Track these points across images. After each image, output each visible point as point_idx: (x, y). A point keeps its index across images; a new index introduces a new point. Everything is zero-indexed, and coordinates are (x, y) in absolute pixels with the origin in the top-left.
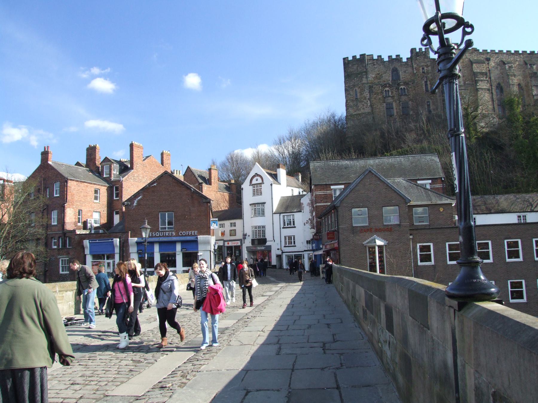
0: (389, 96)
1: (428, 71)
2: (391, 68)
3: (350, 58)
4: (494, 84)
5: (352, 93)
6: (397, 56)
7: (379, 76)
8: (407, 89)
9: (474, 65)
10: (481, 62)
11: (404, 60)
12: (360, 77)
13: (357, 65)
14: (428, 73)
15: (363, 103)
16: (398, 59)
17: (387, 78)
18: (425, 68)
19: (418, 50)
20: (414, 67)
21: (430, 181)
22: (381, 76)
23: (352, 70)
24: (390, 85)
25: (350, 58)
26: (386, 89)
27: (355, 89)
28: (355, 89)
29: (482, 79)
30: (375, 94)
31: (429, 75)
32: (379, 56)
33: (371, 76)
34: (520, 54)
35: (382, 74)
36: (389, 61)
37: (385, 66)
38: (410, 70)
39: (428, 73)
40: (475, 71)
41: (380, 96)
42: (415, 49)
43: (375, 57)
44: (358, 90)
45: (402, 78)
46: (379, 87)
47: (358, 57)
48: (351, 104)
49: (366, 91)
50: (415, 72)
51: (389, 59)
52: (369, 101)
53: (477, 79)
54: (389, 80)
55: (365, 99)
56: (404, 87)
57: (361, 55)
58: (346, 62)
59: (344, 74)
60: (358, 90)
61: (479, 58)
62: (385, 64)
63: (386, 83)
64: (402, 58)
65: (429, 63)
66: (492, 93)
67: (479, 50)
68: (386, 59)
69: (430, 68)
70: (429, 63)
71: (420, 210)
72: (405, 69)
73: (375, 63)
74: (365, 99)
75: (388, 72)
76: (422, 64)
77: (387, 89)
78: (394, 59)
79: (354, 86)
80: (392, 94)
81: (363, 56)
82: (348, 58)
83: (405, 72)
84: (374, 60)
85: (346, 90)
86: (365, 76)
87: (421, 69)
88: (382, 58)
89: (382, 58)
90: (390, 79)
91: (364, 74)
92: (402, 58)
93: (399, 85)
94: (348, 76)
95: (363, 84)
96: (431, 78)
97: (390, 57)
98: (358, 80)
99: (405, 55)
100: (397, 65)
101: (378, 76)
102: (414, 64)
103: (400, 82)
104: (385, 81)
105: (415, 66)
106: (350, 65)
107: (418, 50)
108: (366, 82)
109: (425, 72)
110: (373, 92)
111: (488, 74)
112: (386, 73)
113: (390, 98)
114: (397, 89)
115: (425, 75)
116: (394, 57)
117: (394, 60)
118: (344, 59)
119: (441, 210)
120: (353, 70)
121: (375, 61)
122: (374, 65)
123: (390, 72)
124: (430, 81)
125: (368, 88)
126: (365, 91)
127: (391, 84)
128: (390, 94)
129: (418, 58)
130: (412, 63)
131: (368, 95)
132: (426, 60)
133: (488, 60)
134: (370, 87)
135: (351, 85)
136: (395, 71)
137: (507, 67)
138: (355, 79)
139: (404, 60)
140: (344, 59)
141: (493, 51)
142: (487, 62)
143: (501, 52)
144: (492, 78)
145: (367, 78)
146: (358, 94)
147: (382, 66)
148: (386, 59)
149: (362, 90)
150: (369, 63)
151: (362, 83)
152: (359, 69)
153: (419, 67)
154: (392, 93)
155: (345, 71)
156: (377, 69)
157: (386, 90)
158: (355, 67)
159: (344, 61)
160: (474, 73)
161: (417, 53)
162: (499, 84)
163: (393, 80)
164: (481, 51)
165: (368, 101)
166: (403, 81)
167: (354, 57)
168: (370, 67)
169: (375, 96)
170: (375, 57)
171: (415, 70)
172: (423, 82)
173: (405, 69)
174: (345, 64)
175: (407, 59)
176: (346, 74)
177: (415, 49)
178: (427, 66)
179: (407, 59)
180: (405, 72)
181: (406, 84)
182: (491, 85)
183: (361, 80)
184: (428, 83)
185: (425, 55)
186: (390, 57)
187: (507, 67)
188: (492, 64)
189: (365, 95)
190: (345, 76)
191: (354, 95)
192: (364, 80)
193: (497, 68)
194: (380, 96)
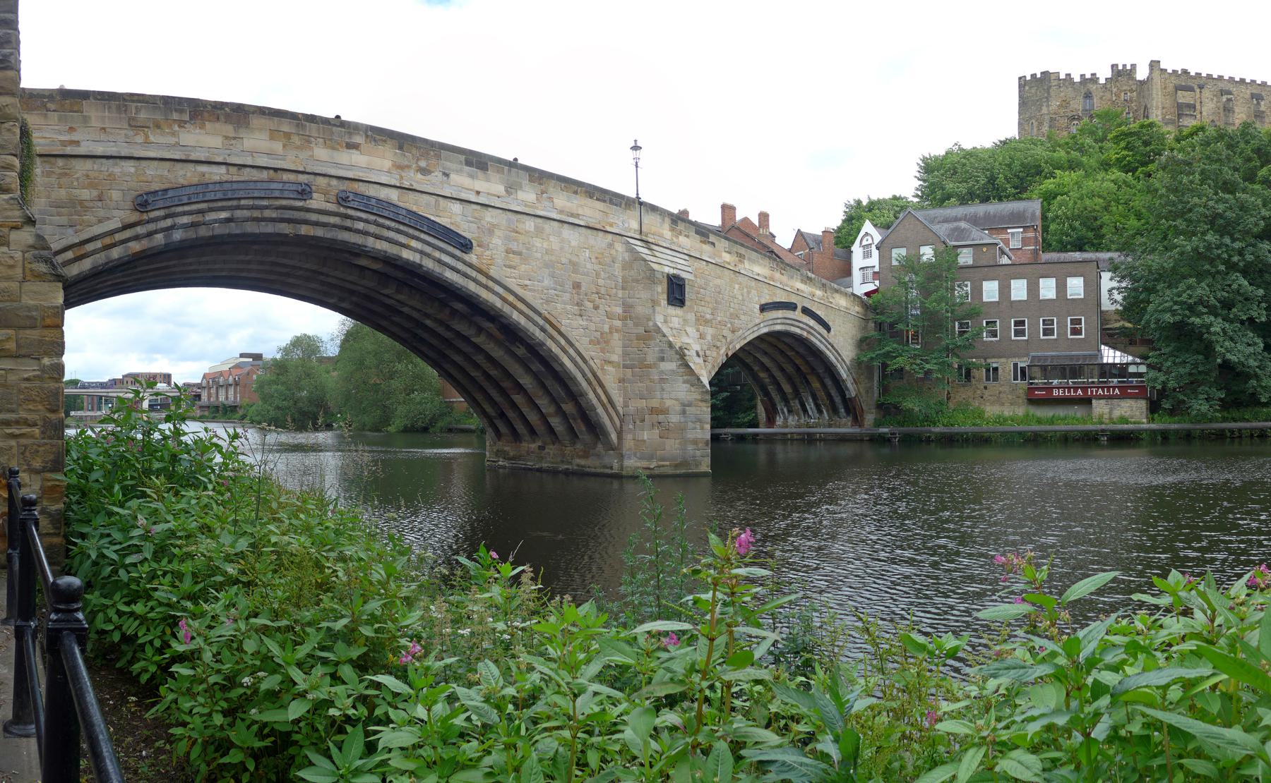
1: (1131, 98)
2: (1083, 91)
3: (1028, 78)
6: (1093, 75)
7: (1065, 103)
10: (1191, 89)
11: (1102, 81)
14: (1131, 101)
17: (1076, 106)
21: (1021, 230)
33: (1054, 104)
36: (1080, 83)
42: (1117, 65)
43: (1062, 76)
44: (1035, 124)
58: (1023, 83)
68: (1077, 79)
70: (1134, 87)
71: (965, 250)
76: (1125, 88)
79: (1031, 118)
81: (1044, 74)
83: (1101, 98)
94: (1023, 103)
97: (1083, 76)
99: (1104, 74)
100: (1093, 87)
106: (1027, 88)
107: (1120, 67)
111: (1198, 107)
116: (1088, 76)
119: (985, 249)
123: (1081, 99)
133: (1201, 87)
134: (1052, 120)
136: (1088, 96)
139: (1102, 81)
142: (1198, 90)
144: (1204, 113)
145: (1048, 106)
148: (1077, 79)
149: (1041, 124)
153: (1121, 91)
158: (1033, 91)
161: (1119, 71)
167: (1033, 76)
168: (1053, 91)
170: (1062, 76)
174: (1020, 86)
177: (1117, 65)
178: (1131, 91)
186: (1083, 76)
187: (1224, 100)
188: (1207, 93)
192: (1044, 110)
193: (1212, 100)
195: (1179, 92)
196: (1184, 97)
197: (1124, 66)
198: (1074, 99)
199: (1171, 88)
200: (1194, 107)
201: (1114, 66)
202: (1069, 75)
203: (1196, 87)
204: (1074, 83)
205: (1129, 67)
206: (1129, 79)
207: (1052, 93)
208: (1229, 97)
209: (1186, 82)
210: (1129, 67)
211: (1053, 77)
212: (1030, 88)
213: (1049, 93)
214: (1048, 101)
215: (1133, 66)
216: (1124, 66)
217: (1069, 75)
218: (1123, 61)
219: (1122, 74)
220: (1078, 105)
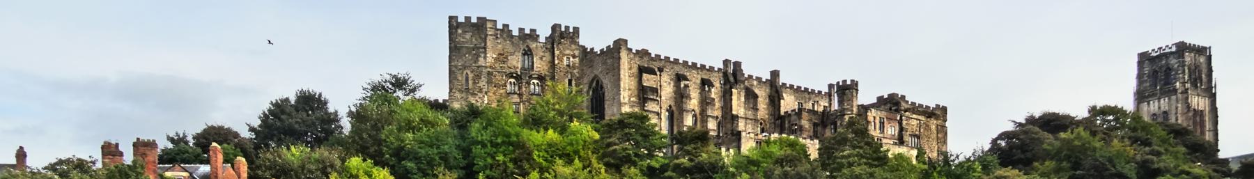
0: (515, 93)
1: (574, 64)
4: (665, 106)
5: (460, 78)
6: (533, 31)
7: (502, 58)
8: (542, 86)
9: (645, 76)
10: (652, 72)
11: (542, 39)
12: (475, 54)
13: (471, 34)
14: (574, 67)
15: (477, 98)
16: (533, 35)
17: (514, 63)
18: (571, 59)
19: (563, 29)
20: (556, 55)
22: (506, 58)
23: (462, 40)
24: (518, 75)
25: (461, 20)
26: (510, 80)
27: (465, 73)
28: (465, 73)
29: (652, 97)
30: (495, 86)
31: (575, 71)
32: (506, 26)
33: (491, 56)
34: (698, 68)
35: (507, 56)
36: (519, 37)
37: (513, 42)
38: (548, 57)
39: (574, 67)
40: (645, 84)
41: (502, 91)
42: (560, 25)
43: (500, 26)
44: (471, 76)
45: (537, 67)
46: (502, 76)
47: (474, 20)
48: (458, 95)
49: (483, 79)
50: (556, 62)
51: (519, 33)
52: (486, 96)
53: (645, 96)
54: (518, 68)
55: (481, 90)
56: (537, 81)
57: (478, 18)
58: (453, 24)
59: (450, 44)
60: (471, 76)
61: (651, 66)
62: (514, 40)
63: (513, 71)
64: (538, 36)
65: (577, 53)
66: (661, 118)
67: (650, 54)
68: (515, 33)
69: (577, 60)
70: (577, 53)
72: (542, 54)
73: (499, 36)
74: (481, 90)
75: (516, 53)
76: (568, 52)
77: (513, 80)
78: (527, 35)
79: (465, 67)
80: (519, 90)
81: (482, 21)
82: (457, 17)
84: (498, 30)
85: (451, 73)
86: (482, 55)
87: (565, 58)
88: (510, 29)
89: (510, 29)
90: (520, 66)
91: (481, 50)
92: (538, 36)
93: (531, 77)
94: (455, 49)
95: (478, 67)
96: (577, 75)
97: (521, 30)
98: (471, 59)
99: (544, 33)
100: (533, 45)
101: (501, 57)
102: (556, 49)
103: (533, 73)
104: (510, 68)
105: (557, 52)
106: (460, 31)
107: (563, 29)
108: (483, 65)
109: (571, 65)
110: (492, 83)
112: (513, 55)
113: (516, 96)
114: (528, 83)
115: (571, 71)
116: (527, 31)
117: (527, 37)
118: (451, 18)
120: (464, 40)
121: (499, 32)
122: (497, 38)
124: (575, 80)
125: (486, 76)
126: (481, 78)
127: (519, 73)
128: (517, 89)
129: (562, 40)
130: (553, 48)
131: (486, 87)
132: (573, 46)
133: (661, 70)
134: (489, 74)
135: (460, 64)
136: (528, 53)
137: (682, 86)
138: (467, 56)
139: (542, 39)
140: (451, 18)
141: (667, 59)
142: (658, 73)
143: (676, 61)
144: (663, 98)
145: (485, 58)
146: (470, 82)
147: (508, 42)
149: (477, 77)
150: (490, 33)
151: (477, 65)
152: (474, 40)
153: (564, 55)
154: (520, 88)
155: (450, 39)
156: (500, 46)
157: (511, 82)
158: (468, 36)
159: (449, 22)
160: (643, 86)
162: (670, 106)
163: (523, 68)
164: (653, 56)
165: (484, 96)
166: (537, 73)
167: (468, 19)
169: (495, 88)
170: (500, 26)
171: (556, 58)
172: (567, 81)
173: (542, 54)
175: (546, 38)
176: (452, 45)
177: (560, 25)
178: (574, 57)
179: (546, 38)
180: (541, 58)
181: (541, 78)
182: (661, 108)
183: (476, 61)
184: (573, 82)
185: (571, 38)
186: (521, 30)
187: (682, 86)
189: (481, 84)
190: (450, 48)
191: (464, 82)
192: (481, 61)
193: (670, 83)
194: (502, 91)
195: (644, 75)
196: (649, 81)
197: (567, 28)
198: (512, 54)
199: (635, 70)
200: (657, 92)
201: (555, 27)
202: (508, 26)
203: (656, 70)
204: (512, 37)
205: (571, 30)
206: (571, 43)
207: (489, 44)
208: (687, 82)
209: (648, 64)
210: (571, 30)
211: (489, 25)
212: (465, 32)
213: (485, 45)
214: (485, 53)
215: (576, 30)
216: (567, 28)
217: (508, 26)
218: (567, 22)
219: (562, 36)
220: (516, 62)
